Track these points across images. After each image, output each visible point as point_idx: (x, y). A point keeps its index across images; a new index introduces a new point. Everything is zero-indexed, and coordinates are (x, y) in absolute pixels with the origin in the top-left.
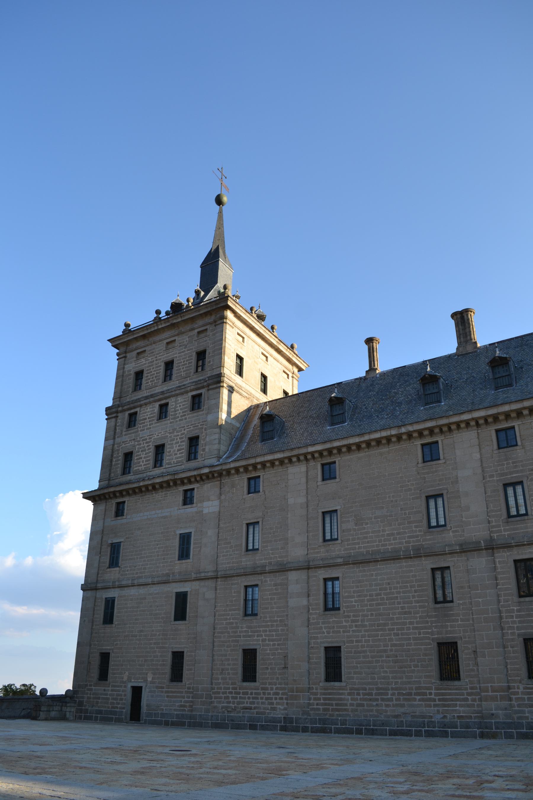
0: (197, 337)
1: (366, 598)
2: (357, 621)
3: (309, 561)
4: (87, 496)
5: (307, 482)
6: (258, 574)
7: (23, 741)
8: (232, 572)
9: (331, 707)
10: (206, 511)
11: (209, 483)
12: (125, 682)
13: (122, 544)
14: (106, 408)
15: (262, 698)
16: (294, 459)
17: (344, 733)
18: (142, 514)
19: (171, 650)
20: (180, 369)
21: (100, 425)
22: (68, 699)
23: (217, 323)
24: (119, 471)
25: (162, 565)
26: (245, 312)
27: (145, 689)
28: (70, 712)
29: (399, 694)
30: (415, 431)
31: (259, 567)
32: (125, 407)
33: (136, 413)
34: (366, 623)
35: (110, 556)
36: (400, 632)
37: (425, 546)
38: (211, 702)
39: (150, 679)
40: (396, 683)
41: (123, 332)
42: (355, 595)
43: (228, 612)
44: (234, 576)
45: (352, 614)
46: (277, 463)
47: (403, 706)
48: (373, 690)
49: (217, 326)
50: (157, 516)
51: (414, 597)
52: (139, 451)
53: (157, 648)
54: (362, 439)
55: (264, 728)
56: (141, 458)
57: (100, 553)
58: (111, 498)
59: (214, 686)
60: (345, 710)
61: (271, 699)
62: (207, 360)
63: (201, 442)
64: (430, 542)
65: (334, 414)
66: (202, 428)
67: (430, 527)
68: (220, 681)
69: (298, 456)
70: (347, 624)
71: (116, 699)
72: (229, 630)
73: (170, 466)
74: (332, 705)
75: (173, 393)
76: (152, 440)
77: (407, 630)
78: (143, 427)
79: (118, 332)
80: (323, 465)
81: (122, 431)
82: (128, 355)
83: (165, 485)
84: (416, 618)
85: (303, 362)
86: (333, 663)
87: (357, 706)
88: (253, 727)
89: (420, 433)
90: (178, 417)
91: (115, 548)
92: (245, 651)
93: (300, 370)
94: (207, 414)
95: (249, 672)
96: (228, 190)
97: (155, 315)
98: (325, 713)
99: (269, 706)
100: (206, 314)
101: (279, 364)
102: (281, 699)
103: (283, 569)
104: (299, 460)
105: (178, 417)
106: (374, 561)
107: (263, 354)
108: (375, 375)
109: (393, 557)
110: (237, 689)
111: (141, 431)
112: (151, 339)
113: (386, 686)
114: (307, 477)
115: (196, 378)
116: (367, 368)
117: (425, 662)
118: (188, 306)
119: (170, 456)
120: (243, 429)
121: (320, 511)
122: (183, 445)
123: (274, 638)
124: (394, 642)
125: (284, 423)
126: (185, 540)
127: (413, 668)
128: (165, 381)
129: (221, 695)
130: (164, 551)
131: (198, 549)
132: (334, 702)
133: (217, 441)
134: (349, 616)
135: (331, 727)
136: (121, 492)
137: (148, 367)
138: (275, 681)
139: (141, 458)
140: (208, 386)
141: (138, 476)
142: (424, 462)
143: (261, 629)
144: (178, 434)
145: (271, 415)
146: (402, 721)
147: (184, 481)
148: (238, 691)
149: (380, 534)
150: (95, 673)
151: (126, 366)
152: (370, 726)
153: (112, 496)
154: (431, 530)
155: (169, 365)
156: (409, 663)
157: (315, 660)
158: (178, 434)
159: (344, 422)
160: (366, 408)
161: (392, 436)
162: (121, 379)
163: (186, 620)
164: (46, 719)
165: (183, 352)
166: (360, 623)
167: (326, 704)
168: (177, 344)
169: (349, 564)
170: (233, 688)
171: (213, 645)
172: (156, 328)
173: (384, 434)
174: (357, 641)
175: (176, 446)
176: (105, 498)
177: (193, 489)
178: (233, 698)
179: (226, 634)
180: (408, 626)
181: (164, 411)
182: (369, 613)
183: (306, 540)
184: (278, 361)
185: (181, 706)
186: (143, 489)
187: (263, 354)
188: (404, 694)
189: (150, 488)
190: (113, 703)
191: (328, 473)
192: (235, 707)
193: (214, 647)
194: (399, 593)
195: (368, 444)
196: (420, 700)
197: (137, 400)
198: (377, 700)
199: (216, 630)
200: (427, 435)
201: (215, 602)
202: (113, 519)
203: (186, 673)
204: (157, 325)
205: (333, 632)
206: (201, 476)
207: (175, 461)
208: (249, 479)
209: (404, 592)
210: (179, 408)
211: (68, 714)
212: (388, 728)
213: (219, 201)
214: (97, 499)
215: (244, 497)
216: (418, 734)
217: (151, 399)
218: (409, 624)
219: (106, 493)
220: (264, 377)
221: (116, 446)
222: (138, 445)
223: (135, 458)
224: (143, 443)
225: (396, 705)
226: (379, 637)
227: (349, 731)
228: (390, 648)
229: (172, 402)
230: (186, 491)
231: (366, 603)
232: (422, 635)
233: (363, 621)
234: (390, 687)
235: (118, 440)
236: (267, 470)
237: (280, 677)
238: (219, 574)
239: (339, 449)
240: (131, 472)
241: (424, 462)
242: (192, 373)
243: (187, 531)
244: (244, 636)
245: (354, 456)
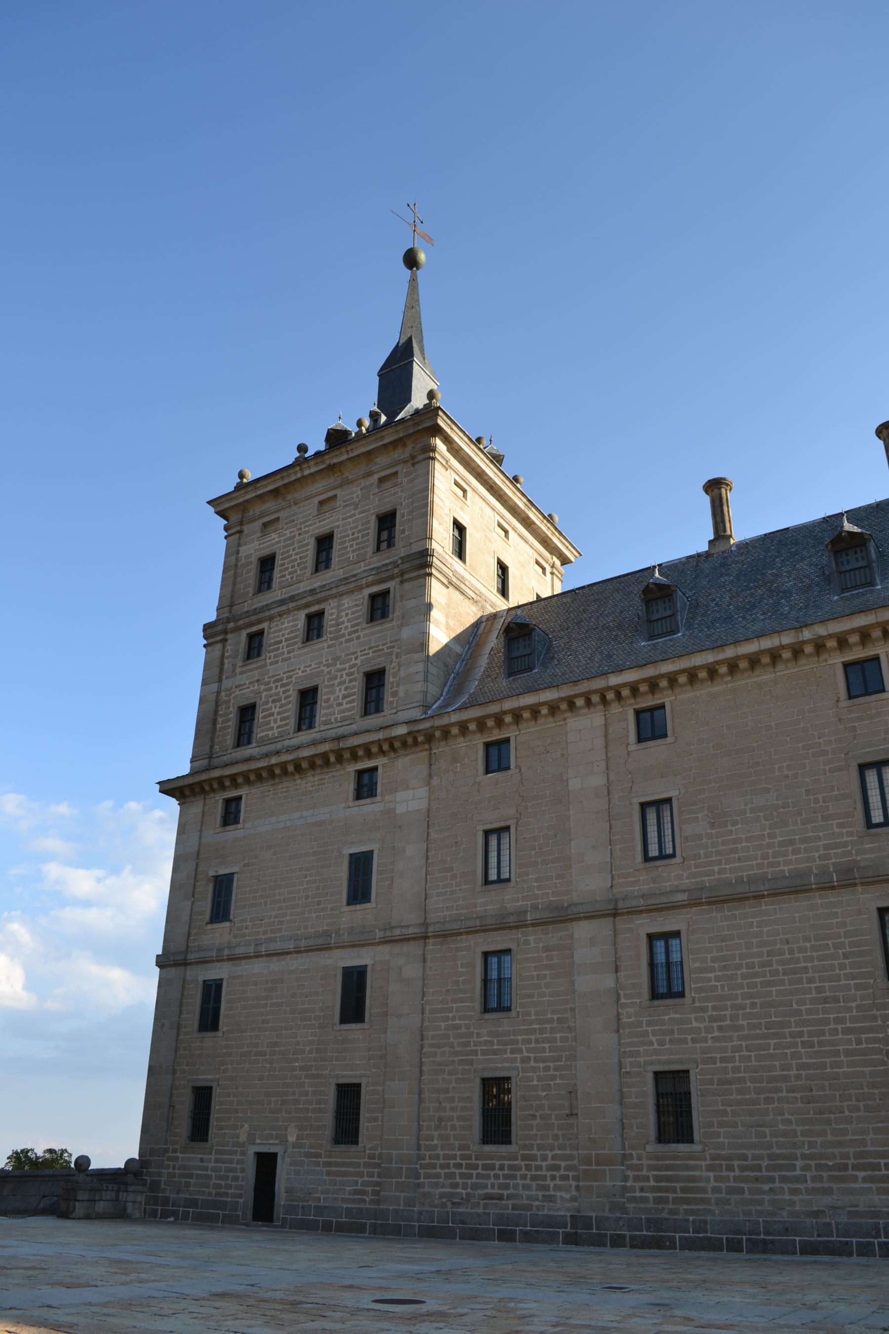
0: (379, 487)
1: (739, 972)
2: (722, 1018)
3: (616, 901)
4: (169, 788)
5: (606, 747)
6: (510, 928)
7: (31, 1273)
8: (456, 926)
9: (671, 1196)
10: (401, 809)
11: (406, 755)
12: (242, 1145)
13: (236, 876)
14: (205, 625)
15: (524, 1177)
16: (580, 702)
17: (703, 1248)
18: (273, 820)
19: (334, 1081)
20: (346, 548)
21: (194, 656)
22: (130, 1178)
23: (416, 460)
24: (230, 740)
25: (314, 915)
26: (468, 442)
27: (283, 1159)
28: (134, 1202)
29: (819, 1167)
30: (830, 636)
31: (512, 914)
32: (241, 622)
33: (261, 633)
34: (741, 1022)
35: (213, 901)
36: (816, 1039)
37: (862, 865)
38: (418, 1185)
39: (292, 1139)
40: (812, 1145)
42: (716, 965)
43: (450, 1005)
44: (460, 934)
45: (710, 1004)
46: (544, 711)
47: (827, 1192)
48: (763, 1159)
49: (417, 466)
50: (300, 826)
51: (842, 967)
52: (268, 702)
53: (306, 1077)
54: (721, 656)
55: (529, 1238)
56: (272, 715)
57: (193, 896)
58: (213, 790)
59: (423, 1152)
60: (703, 1201)
61: (544, 1178)
62: (398, 527)
63: (389, 679)
64: (873, 856)
65: (652, 619)
66: (391, 653)
67: (870, 825)
68: (436, 1142)
70: (702, 1025)
71: (225, 1178)
72: (451, 1040)
73: (329, 727)
74: (675, 1192)
75: (334, 591)
76: (293, 679)
77: (830, 1035)
78: (276, 656)
79: (229, 486)
80: (638, 713)
82: (246, 528)
83: (319, 762)
84: (850, 1010)
86: (674, 1106)
87: (728, 1193)
88: (506, 1236)
89: (842, 642)
90: (344, 635)
91: (223, 886)
92: (486, 1082)
93: (565, 561)
94: (400, 627)
95: (496, 1123)
97: (298, 455)
98: (660, 1206)
99: (540, 1194)
100: (394, 444)
101: (528, 547)
102: (565, 1178)
103: (562, 916)
104: (589, 703)
105: (344, 635)
106: (755, 897)
107: (500, 525)
108: (727, 547)
109: (796, 888)
110: (470, 1159)
111: (271, 664)
112: (289, 497)
113: (790, 1151)
114: (606, 736)
115: (377, 561)
116: (711, 537)
117: (875, 1099)
118: (359, 433)
119: (328, 708)
120: (468, 657)
121: (637, 801)
122: (354, 687)
123: (547, 1054)
124: (804, 1060)
125: (551, 642)
126: (361, 867)
127: (847, 1113)
128: (317, 571)
129: (438, 1170)
130: (318, 888)
131: (387, 883)
132: (678, 1185)
133: (421, 677)
134: (703, 1009)
135: (674, 1237)
136: (233, 778)
137: (284, 547)
138: (551, 1141)
139: (272, 715)
140: (402, 574)
141: (265, 749)
142: (850, 697)
143: (519, 1038)
144: (343, 666)
145: (527, 625)
146: (829, 1224)
147: (357, 753)
148: (474, 1162)
149: (764, 843)
150: (183, 1125)
151: (241, 549)
152: (759, 1234)
153: (215, 786)
154: (873, 831)
155: (325, 543)
156: (838, 1104)
157: (634, 1099)
158: (343, 666)
159: (673, 632)
160: (717, 605)
161: (783, 647)
162: (232, 572)
163: (363, 1021)
164: (87, 1217)
165: (351, 517)
166: (728, 1022)
167: (660, 1189)
168: (339, 502)
169: (701, 904)
170: (463, 1157)
171: (421, 1071)
172: (299, 475)
173: (767, 643)
174: (723, 1060)
175: (340, 690)
176: (203, 791)
177: (375, 769)
178: (462, 1176)
179: (447, 1049)
180: (832, 1026)
181: (316, 626)
182: (748, 1002)
183: (608, 859)
184: (526, 541)
185: (356, 1192)
186: (277, 771)
187: (500, 525)
188: (830, 1168)
189: (291, 768)
190: (219, 1186)
191: (650, 726)
192: (467, 1194)
193: (421, 1076)
194: (811, 959)
195: (733, 667)
196: (865, 1180)
197: (263, 607)
198: (771, 1180)
199: (425, 1042)
200: (856, 644)
201: (424, 985)
202: (218, 830)
203: (365, 1126)
204: (301, 470)
205: (671, 1041)
206: (391, 741)
207: (339, 716)
208: (488, 746)
209: (820, 958)
210: (345, 619)
211: (130, 1206)
212: (797, 1239)
213: (411, 260)
214: (187, 792)
215: (478, 779)
216: (865, 1250)
217: (291, 605)
218: (835, 1023)
219: (205, 781)
220: (503, 569)
221: (223, 694)
222: (265, 690)
223: (261, 715)
224: (276, 687)
225: (815, 1191)
226: (772, 1051)
227: (713, 1245)
228: (795, 1072)
229: (332, 608)
230: (360, 773)
231: (740, 981)
232: (864, 1046)
233: (734, 1018)
234: (798, 1152)
235: (226, 683)
236: (523, 725)
237: (560, 1133)
238: (431, 929)
239: (672, 679)
240: (254, 741)
241: (850, 697)
242: (370, 554)
243: (365, 848)
244: (484, 1053)
245: (704, 691)
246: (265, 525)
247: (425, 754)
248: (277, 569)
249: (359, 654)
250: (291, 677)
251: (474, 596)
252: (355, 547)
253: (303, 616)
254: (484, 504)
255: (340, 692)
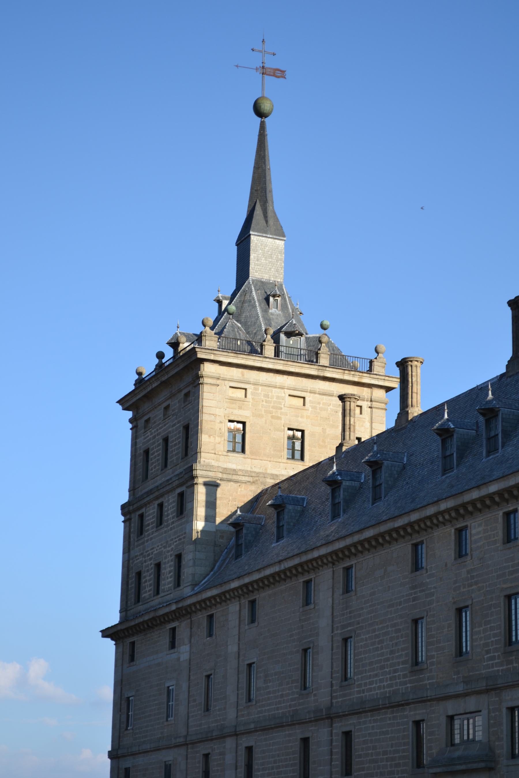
0: (185, 401)
4: (107, 633)
26: (235, 355)
32: (135, 506)
41: (135, 385)
50: (177, 657)
56: (146, 582)
57: (120, 711)
69: (228, 591)
81: (134, 539)
85: (387, 378)
96: (279, 73)
97: (157, 361)
111: (147, 541)
114: (240, 618)
133: (191, 563)
140: (187, 481)
151: (138, 440)
168: (170, 412)
210: (169, 512)
217: (152, 497)
221: (131, 561)
246: (147, 421)
247: (189, 620)
248: (150, 462)
249: (174, 540)
250: (152, 553)
251: (251, 479)
252: (176, 452)
253: (156, 505)
254: (270, 388)
255: (168, 570)
